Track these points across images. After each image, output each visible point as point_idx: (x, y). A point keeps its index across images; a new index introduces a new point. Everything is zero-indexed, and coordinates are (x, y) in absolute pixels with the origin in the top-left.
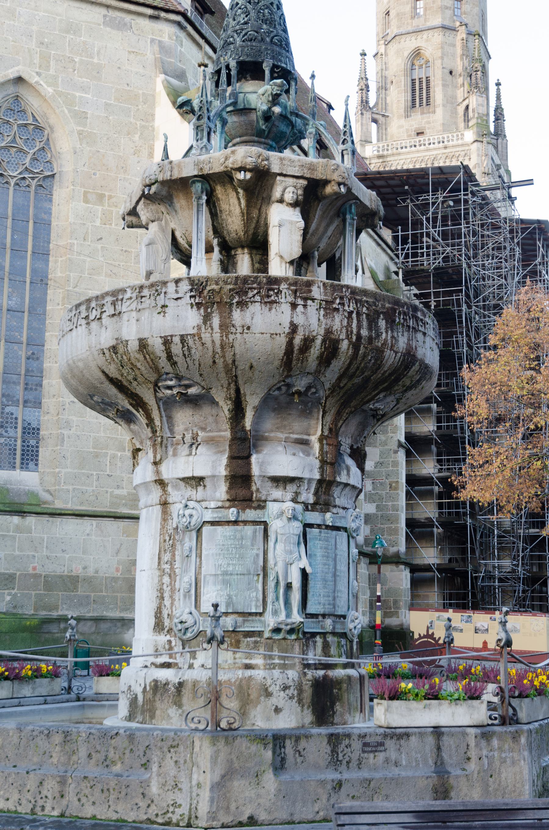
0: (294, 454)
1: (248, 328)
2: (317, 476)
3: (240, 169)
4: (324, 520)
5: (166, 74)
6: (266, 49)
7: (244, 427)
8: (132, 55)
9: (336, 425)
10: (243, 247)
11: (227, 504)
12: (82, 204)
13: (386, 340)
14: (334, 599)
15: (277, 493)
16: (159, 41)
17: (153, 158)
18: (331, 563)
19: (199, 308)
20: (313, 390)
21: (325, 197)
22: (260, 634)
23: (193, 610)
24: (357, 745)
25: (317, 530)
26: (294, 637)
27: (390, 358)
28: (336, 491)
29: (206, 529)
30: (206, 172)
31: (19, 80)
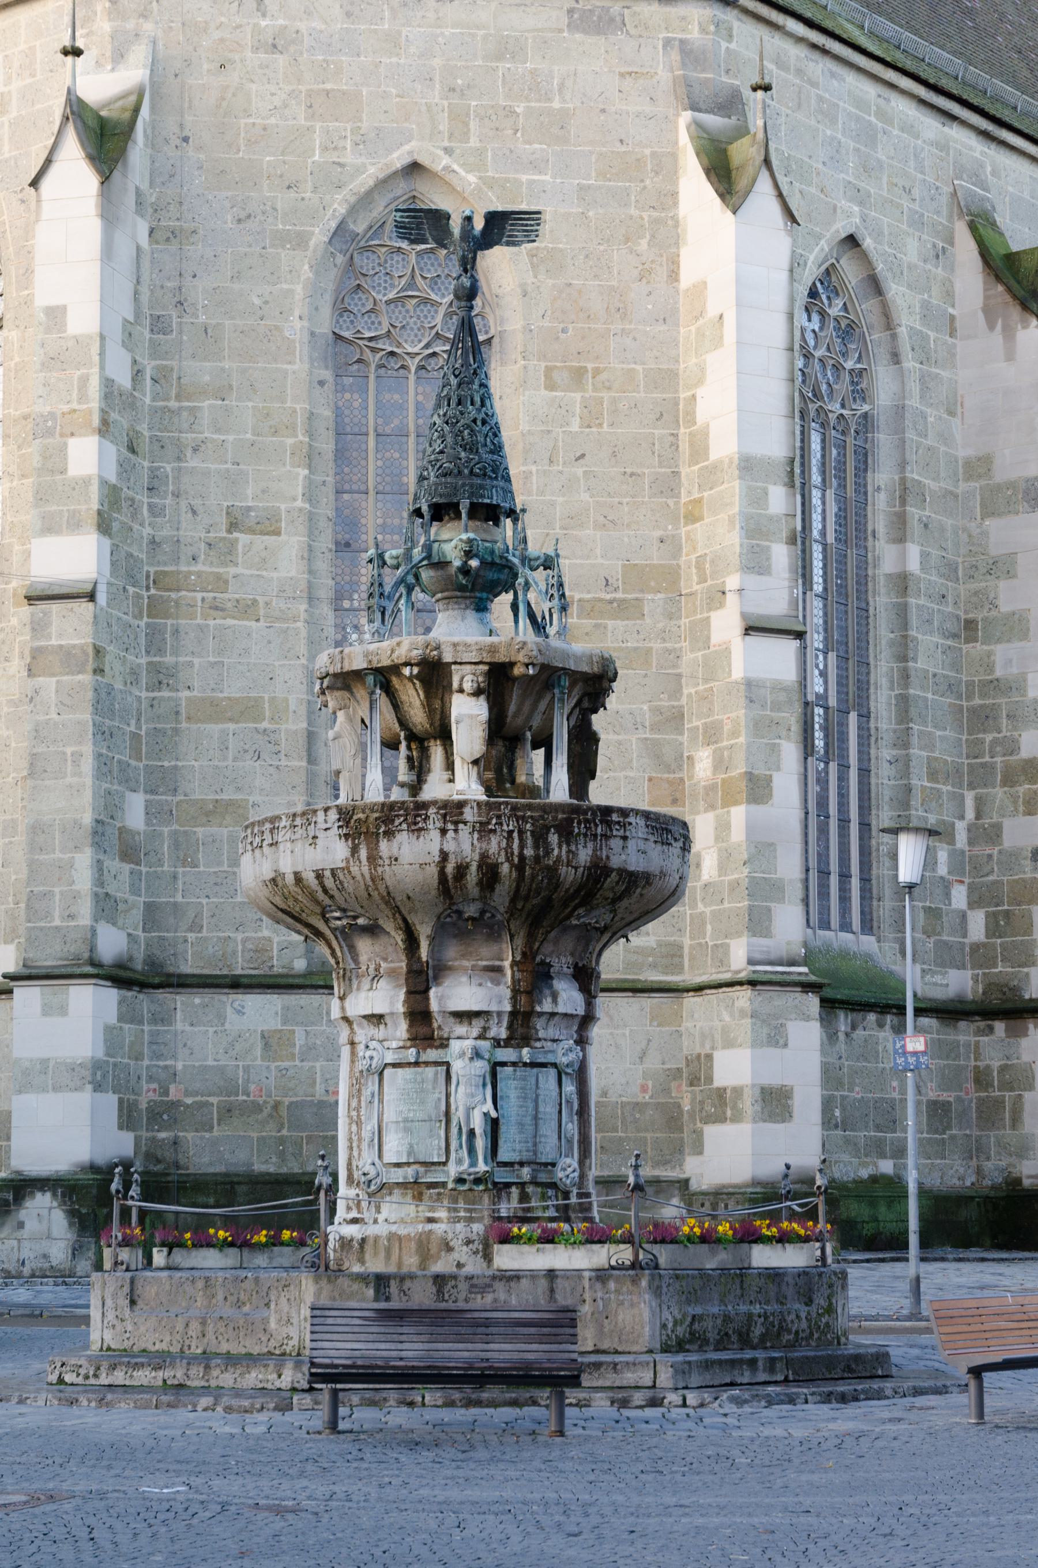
0: (480, 985)
1: (396, 859)
2: (508, 1007)
3: (406, 664)
4: (521, 1057)
5: (694, 108)
6: (464, 485)
7: (419, 958)
8: (629, 79)
9: (531, 948)
10: (435, 738)
11: (409, 1044)
13: (559, 856)
14: (535, 1145)
15: (461, 1030)
16: (682, 42)
17: (677, 280)
18: (531, 1105)
19: (347, 840)
20: (488, 915)
21: (514, 679)
22: (444, 1184)
23: (377, 1160)
24: (463, 1286)
25: (511, 1069)
26: (481, 1187)
27: (568, 875)
28: (539, 1023)
29: (387, 1072)
30: (375, 665)
31: (414, 168)
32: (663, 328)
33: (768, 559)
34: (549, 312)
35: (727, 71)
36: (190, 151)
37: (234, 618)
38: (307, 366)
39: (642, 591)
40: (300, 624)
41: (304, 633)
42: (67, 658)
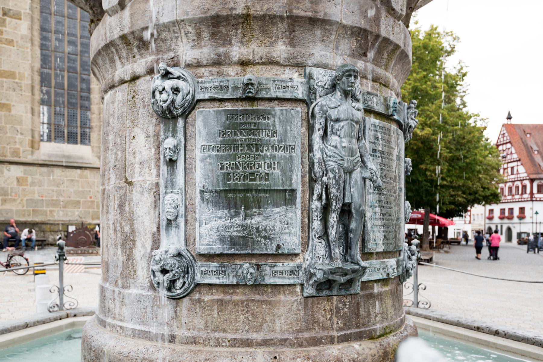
37: (5, 44)
40: (29, 50)
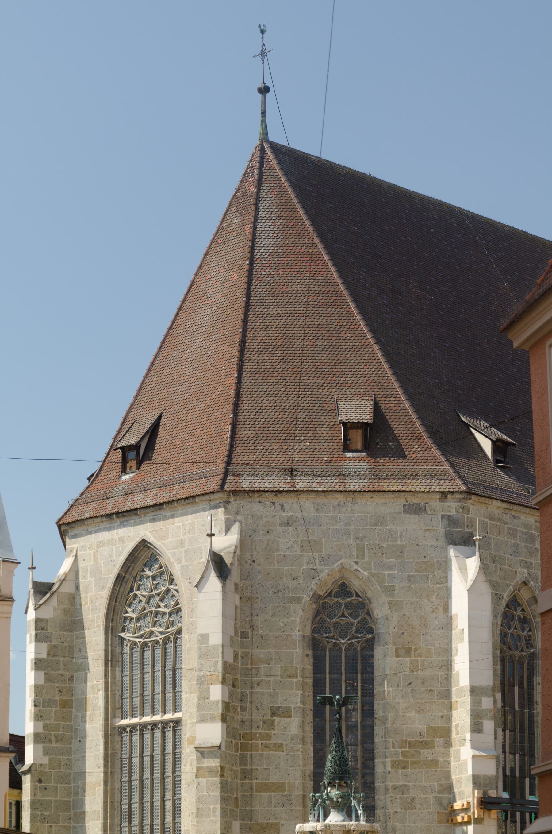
12: (395, 658)
16: (449, 516)
32: (442, 631)
33: (482, 727)
34: (397, 626)
35: (467, 526)
36: (255, 566)
37: (273, 751)
38: (301, 650)
39: (434, 737)
40: (299, 753)
41: (301, 756)
42: (210, 771)
